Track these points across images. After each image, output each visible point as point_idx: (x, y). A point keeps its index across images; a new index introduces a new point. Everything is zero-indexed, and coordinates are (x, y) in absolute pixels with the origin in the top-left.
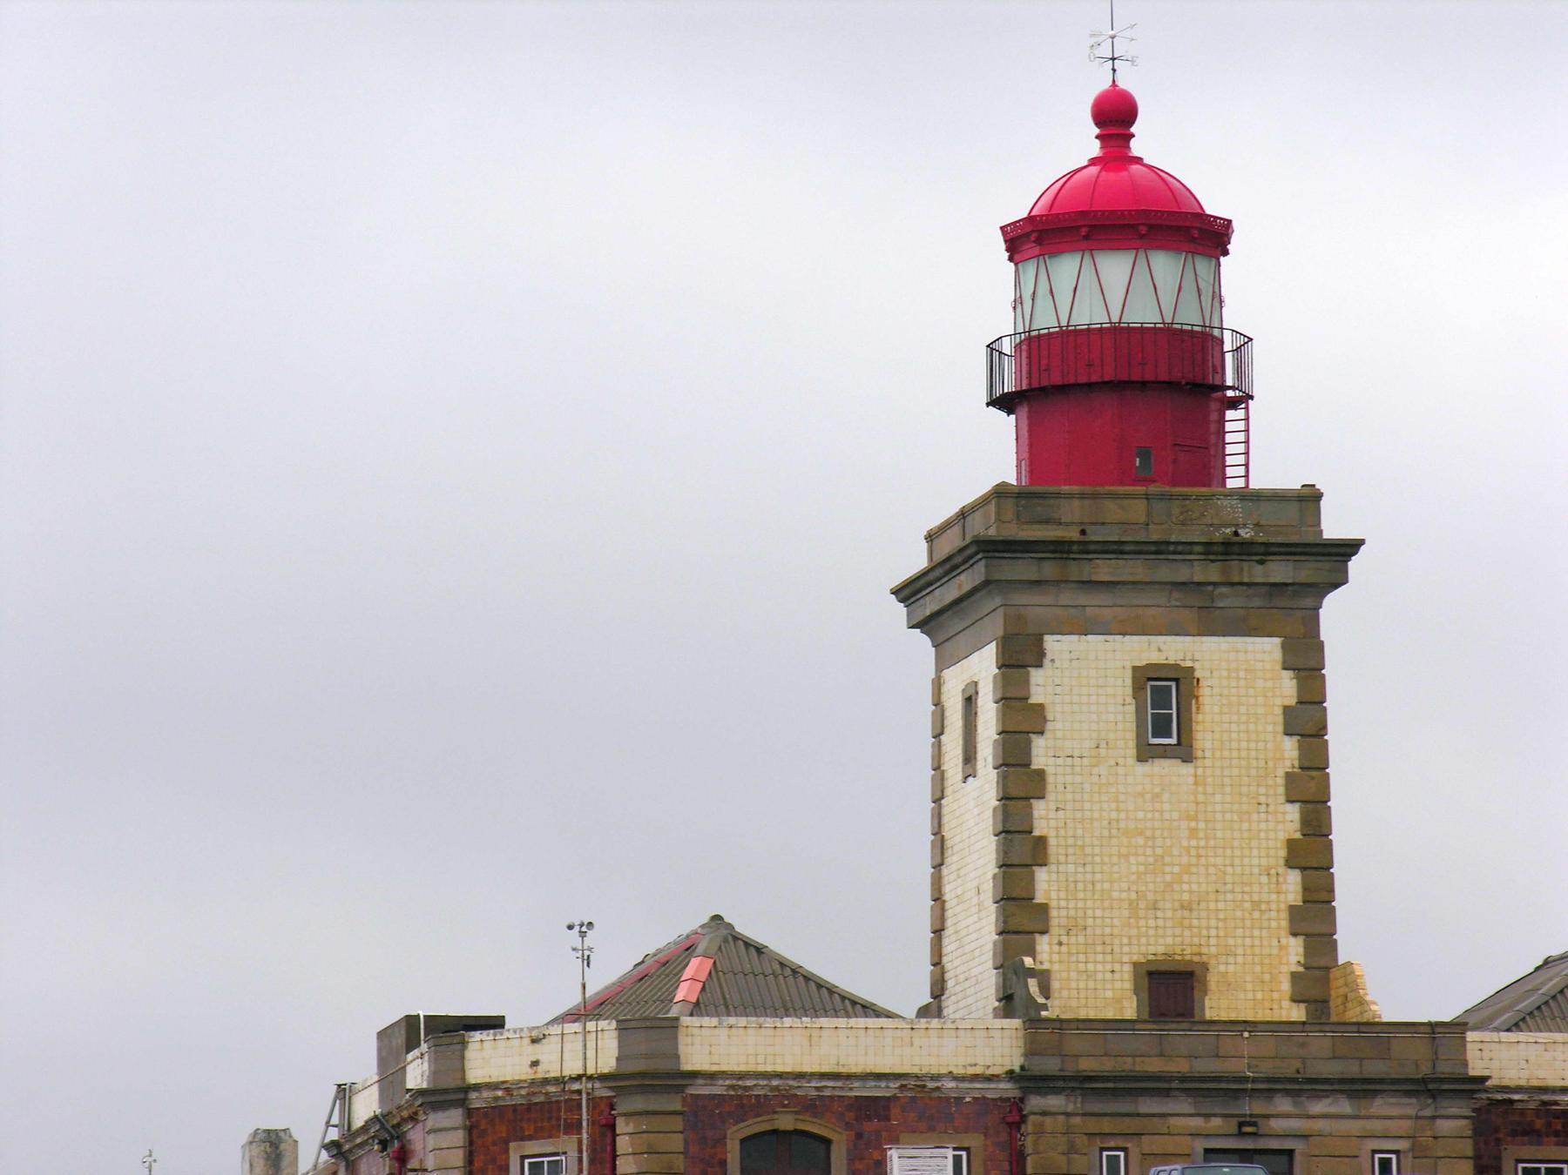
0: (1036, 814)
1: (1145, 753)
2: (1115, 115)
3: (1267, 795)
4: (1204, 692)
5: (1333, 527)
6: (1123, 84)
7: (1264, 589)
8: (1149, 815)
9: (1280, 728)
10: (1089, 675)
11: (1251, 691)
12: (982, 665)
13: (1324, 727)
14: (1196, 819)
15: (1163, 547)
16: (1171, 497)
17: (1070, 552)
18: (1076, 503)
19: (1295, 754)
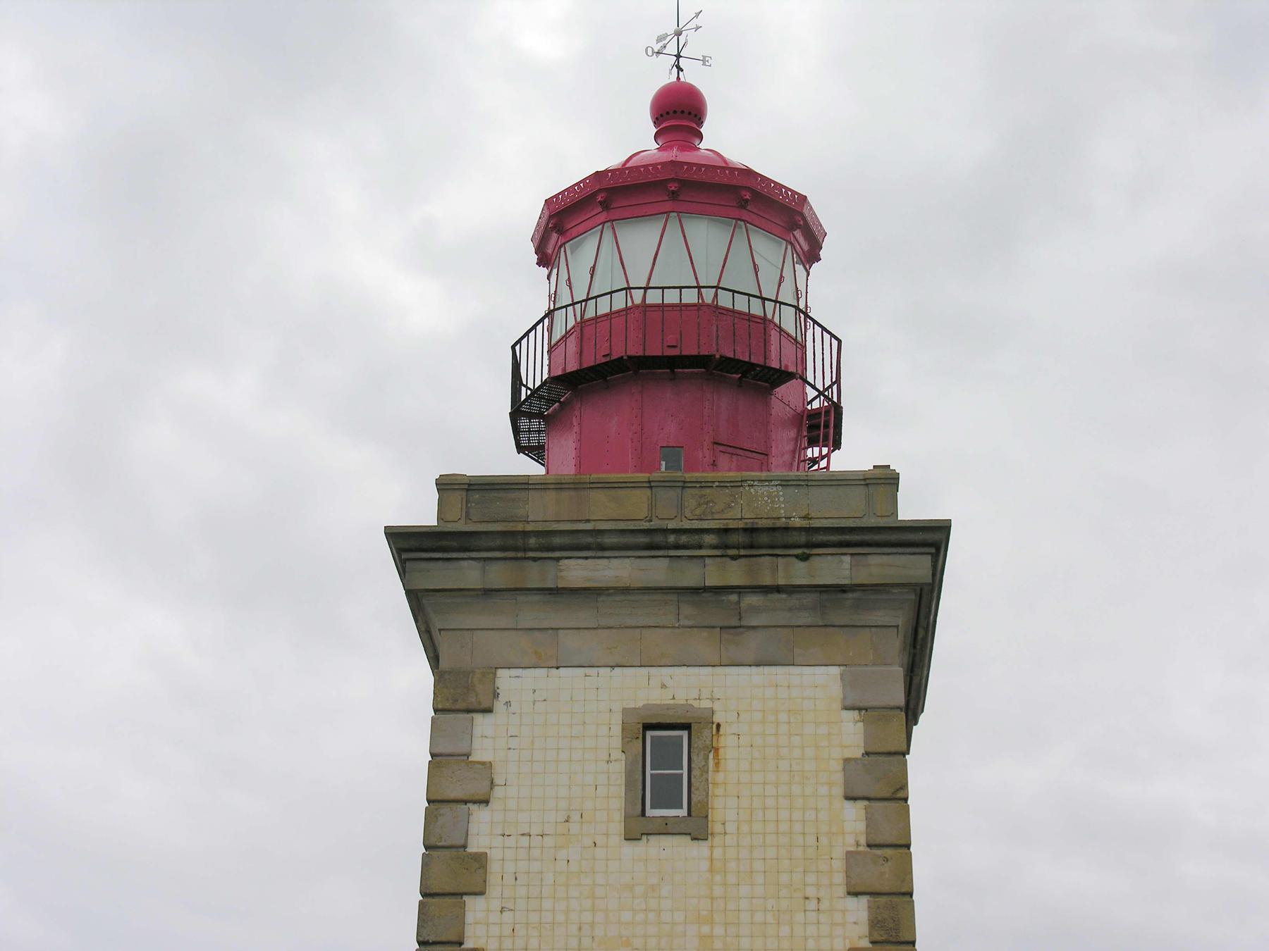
0: (470, 917)
1: (638, 828)
2: (679, 111)
3: (818, 886)
4: (727, 742)
6: (689, 77)
7: (809, 599)
8: (640, 917)
9: (839, 791)
11: (796, 740)
13: (904, 786)
14: (711, 923)
15: (658, 539)
16: (684, 485)
17: (525, 550)
18: (551, 496)
19: (861, 826)
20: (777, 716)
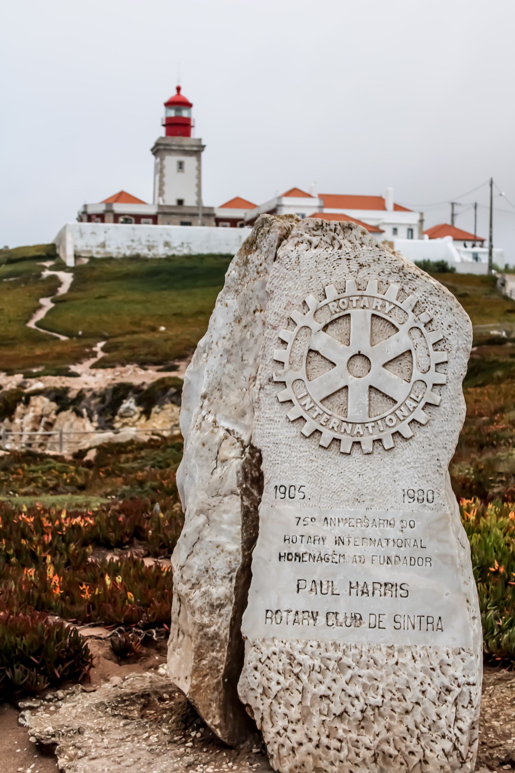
2: (178, 89)
5: (203, 143)
10: (171, 161)
12: (158, 160)
20: (190, 162)
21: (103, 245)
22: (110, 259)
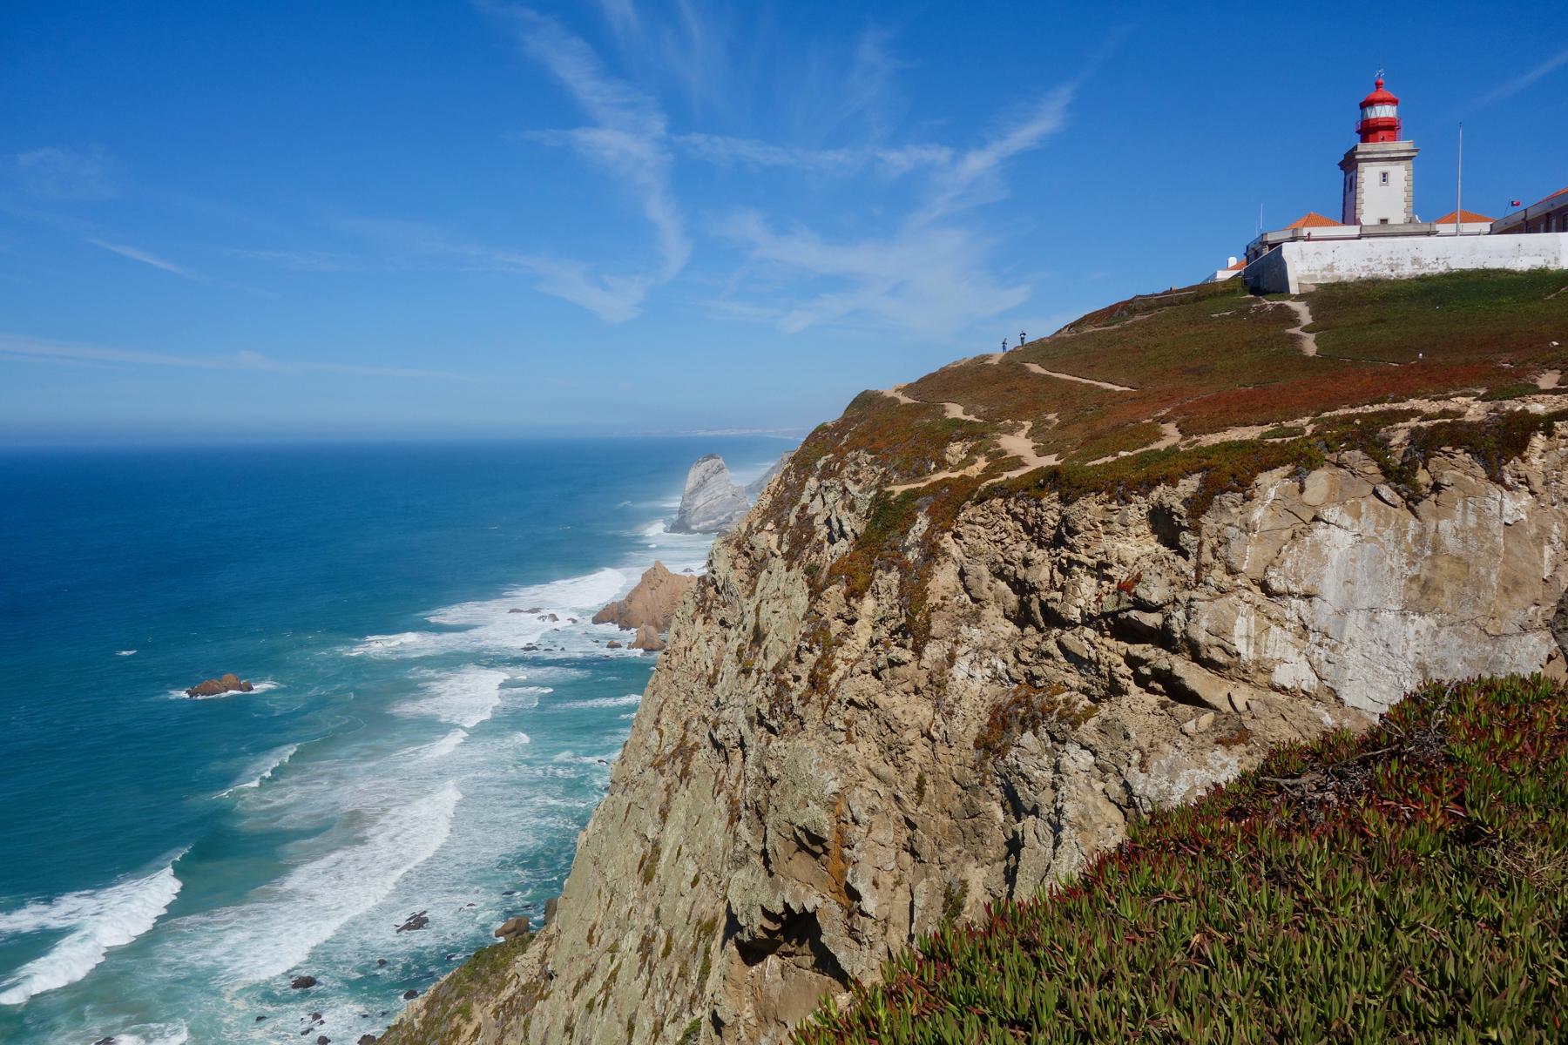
21: (1331, 268)
22: (1342, 285)
